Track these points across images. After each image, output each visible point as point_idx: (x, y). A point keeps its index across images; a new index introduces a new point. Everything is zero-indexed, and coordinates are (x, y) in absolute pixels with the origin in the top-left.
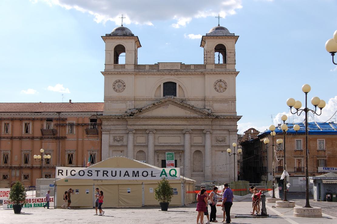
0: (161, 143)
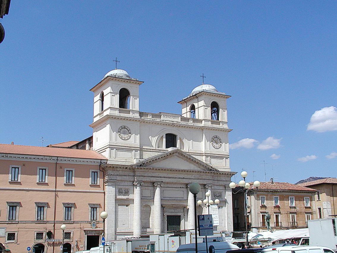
0: (165, 197)
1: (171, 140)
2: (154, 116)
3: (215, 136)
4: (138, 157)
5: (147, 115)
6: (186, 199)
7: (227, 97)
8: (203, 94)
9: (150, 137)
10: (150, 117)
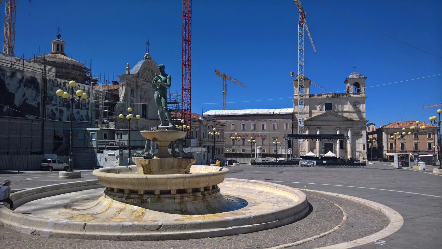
1: (329, 107)
2: (318, 95)
4: (308, 116)
5: (314, 96)
7: (365, 78)
9: (316, 106)
10: (316, 97)
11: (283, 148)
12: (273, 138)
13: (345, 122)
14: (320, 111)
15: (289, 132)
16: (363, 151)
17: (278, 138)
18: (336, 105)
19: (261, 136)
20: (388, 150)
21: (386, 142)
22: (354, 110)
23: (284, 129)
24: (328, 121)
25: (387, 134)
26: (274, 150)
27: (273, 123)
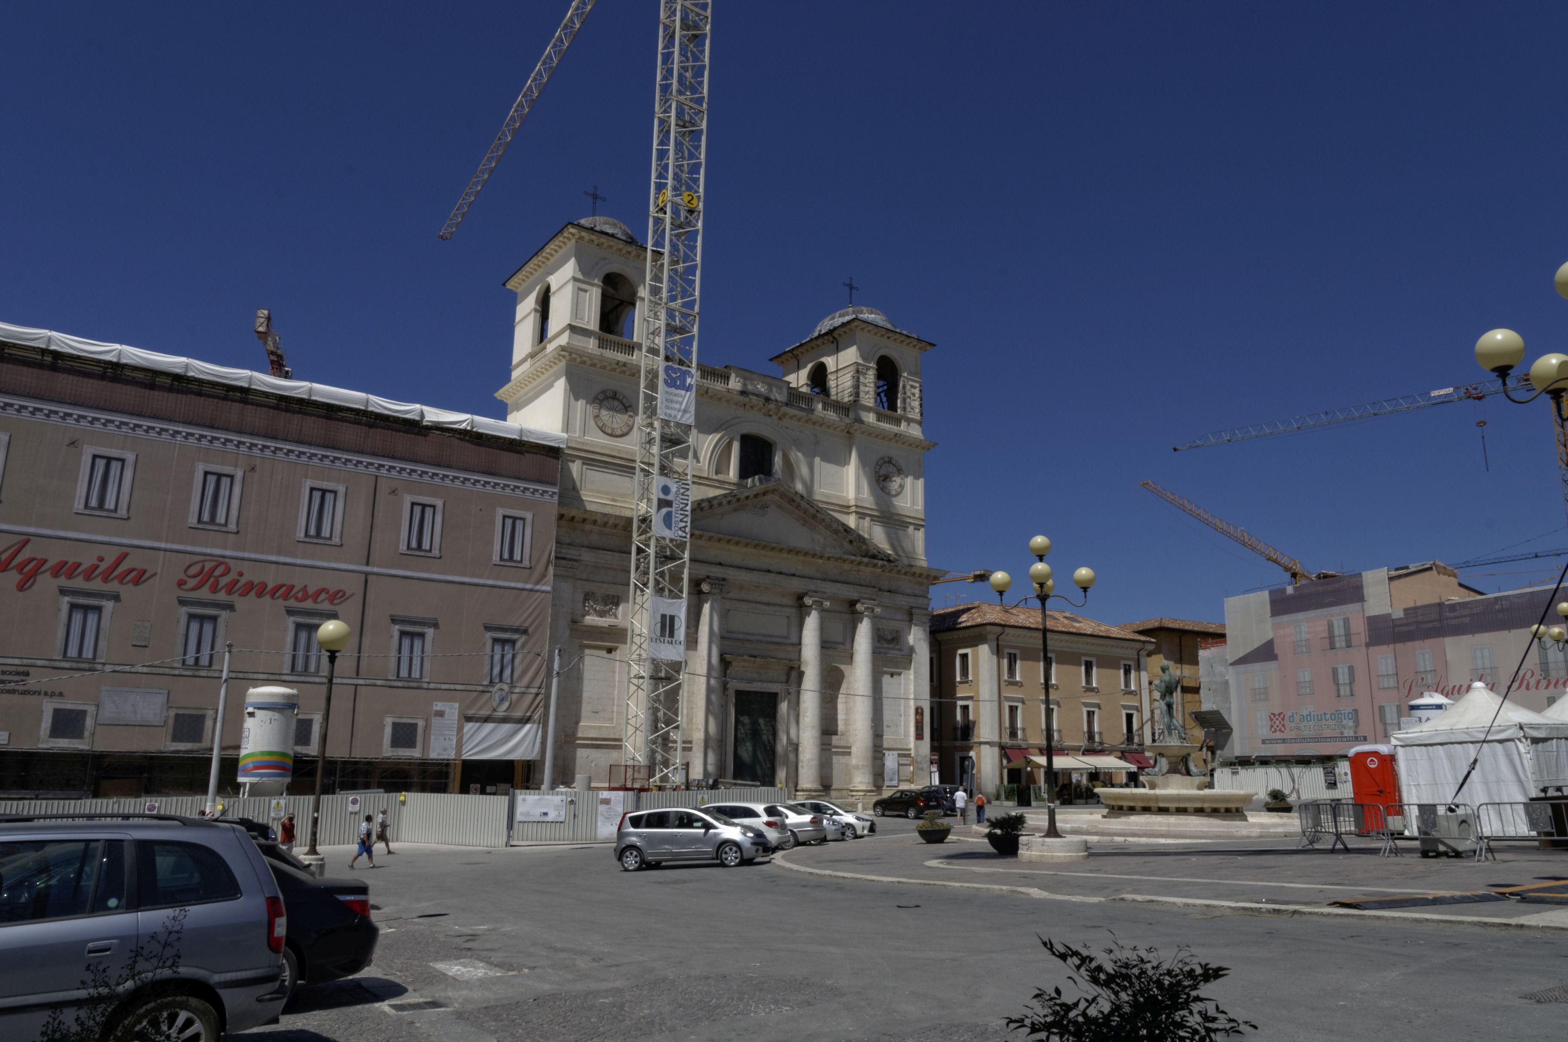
3: (886, 459)
6: (794, 640)
8: (857, 327)
11: (471, 712)
12: (394, 620)
13: (852, 562)
14: (717, 473)
15: (529, 586)
16: (916, 747)
17: (435, 625)
18: (798, 457)
19: (286, 597)
20: (1003, 741)
21: (996, 697)
22: (877, 504)
23: (496, 558)
24: (759, 544)
25: (998, 652)
26: (395, 725)
27: (408, 499)
